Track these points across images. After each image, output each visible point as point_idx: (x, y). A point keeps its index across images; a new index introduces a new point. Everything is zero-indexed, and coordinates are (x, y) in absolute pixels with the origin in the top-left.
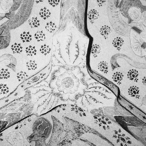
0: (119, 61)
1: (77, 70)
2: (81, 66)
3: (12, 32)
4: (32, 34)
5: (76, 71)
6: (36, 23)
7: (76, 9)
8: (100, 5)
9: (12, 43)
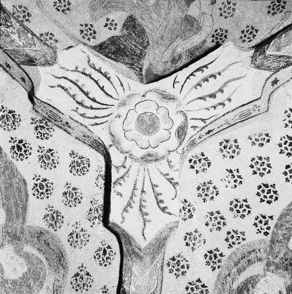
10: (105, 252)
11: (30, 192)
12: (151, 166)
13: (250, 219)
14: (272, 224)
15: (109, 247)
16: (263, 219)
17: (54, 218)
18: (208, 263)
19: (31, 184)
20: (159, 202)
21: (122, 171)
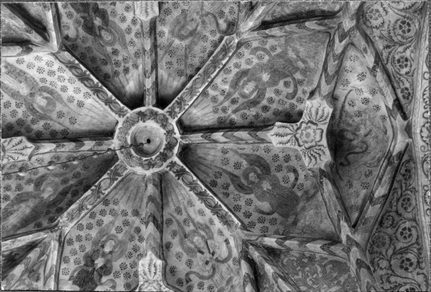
0: (192, 276)
1: (156, 283)
2: (159, 279)
3: (114, 264)
4: (128, 263)
5: (155, 285)
6: (130, 255)
7: (152, 243)
8: (174, 238)
9: (113, 271)
10: (39, 161)
11: (22, 192)
12: (6, 149)
13: (18, 110)
14: (18, 102)
15: (37, 160)
16: (18, 105)
17: (29, 181)
18: (36, 123)
19: (18, 192)
20: (19, 144)
21: (10, 158)
